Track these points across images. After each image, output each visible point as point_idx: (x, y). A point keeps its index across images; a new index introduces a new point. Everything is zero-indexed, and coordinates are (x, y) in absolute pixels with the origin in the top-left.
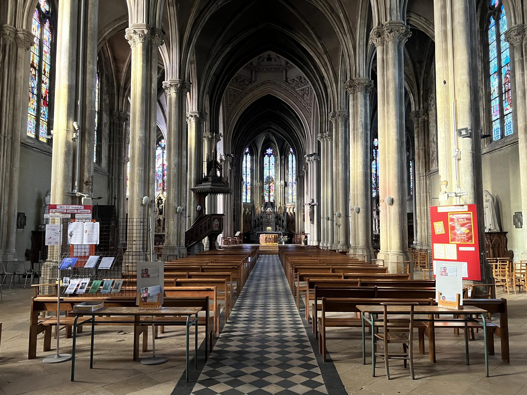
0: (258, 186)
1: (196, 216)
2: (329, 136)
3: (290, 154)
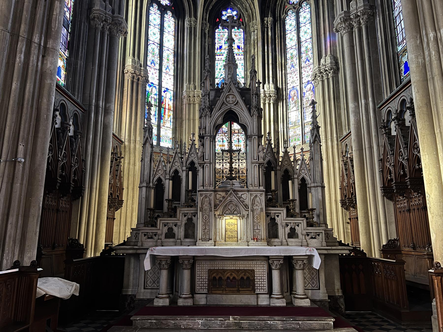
3: (290, 12)
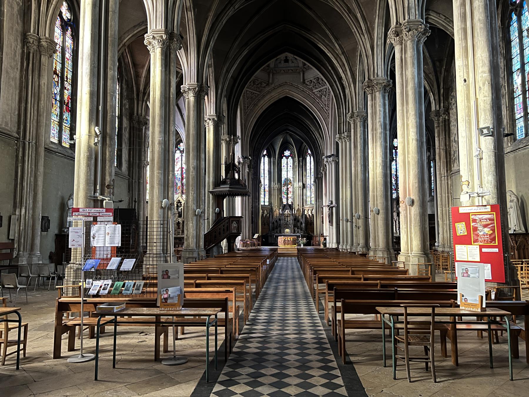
0: (276, 189)
1: (214, 218)
2: (347, 137)
3: (308, 156)
